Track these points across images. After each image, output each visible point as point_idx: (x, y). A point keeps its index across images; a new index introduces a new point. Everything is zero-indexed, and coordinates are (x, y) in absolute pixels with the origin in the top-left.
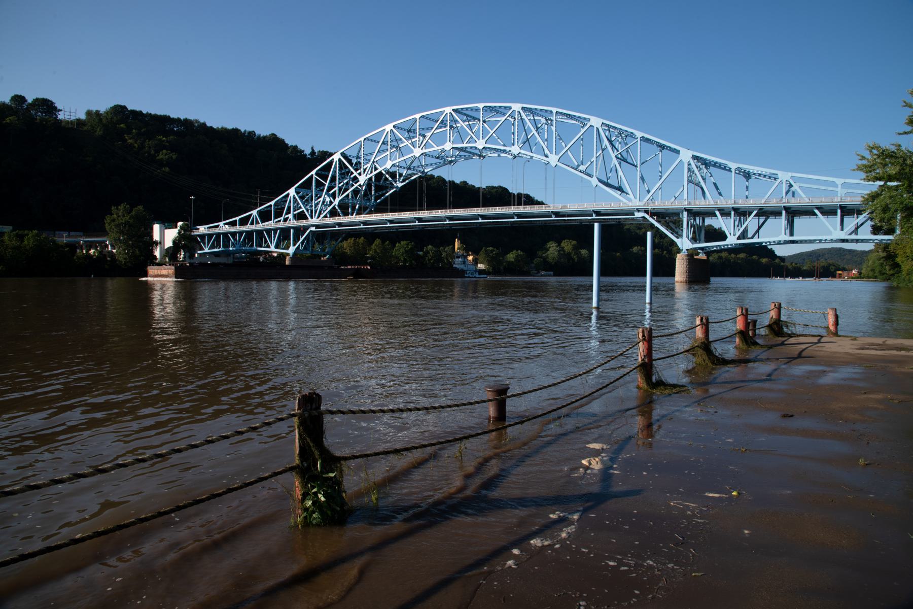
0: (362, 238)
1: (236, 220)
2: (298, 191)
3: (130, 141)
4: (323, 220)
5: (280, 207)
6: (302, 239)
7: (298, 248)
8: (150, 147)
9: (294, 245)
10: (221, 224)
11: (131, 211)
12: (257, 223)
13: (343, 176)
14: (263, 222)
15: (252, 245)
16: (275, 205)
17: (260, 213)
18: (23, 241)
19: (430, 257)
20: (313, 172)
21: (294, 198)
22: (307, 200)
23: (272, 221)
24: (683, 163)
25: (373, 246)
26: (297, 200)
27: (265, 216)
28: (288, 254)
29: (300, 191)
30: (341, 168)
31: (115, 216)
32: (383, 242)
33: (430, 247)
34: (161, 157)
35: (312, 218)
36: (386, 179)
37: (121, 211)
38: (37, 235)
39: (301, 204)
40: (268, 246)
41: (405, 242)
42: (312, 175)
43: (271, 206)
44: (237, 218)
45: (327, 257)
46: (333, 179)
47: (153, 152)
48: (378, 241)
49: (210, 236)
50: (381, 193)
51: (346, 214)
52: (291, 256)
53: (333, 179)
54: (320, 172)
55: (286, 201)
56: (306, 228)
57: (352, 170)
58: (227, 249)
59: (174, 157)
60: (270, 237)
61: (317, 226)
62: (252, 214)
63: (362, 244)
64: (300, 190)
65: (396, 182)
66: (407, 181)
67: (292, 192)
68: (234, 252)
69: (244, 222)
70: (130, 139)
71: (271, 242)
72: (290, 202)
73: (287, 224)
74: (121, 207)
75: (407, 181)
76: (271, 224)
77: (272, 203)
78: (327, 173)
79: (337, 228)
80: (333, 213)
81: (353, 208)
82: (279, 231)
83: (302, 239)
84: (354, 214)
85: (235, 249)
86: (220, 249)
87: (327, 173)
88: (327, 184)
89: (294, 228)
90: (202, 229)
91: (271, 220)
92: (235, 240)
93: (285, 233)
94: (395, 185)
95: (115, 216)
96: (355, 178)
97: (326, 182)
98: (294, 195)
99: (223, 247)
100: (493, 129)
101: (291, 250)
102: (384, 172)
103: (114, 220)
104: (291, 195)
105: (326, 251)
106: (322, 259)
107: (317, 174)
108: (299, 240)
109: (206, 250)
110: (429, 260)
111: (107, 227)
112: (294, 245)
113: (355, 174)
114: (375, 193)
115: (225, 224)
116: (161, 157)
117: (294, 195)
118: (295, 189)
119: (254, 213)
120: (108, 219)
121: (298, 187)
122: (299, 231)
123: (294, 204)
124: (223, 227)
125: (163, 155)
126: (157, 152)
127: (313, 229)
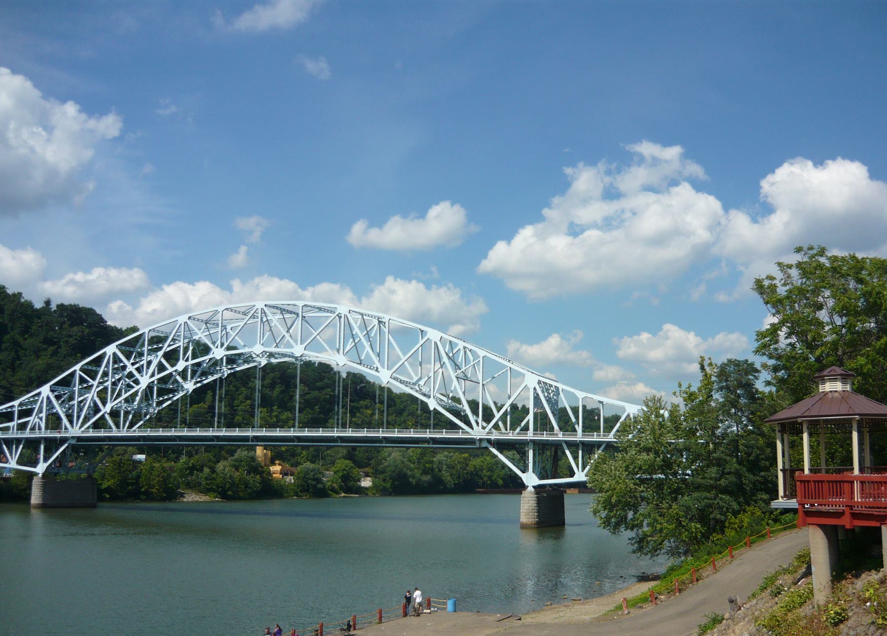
2: (53, 389)
9: (45, 460)
13: (115, 371)
16: (21, 405)
20: (77, 367)
21: (48, 398)
22: (63, 402)
24: (529, 389)
28: (36, 474)
30: (115, 362)
42: (74, 372)
50: (166, 397)
54: (86, 367)
72: (42, 402)
73: (36, 435)
77: (16, 403)
88: (95, 383)
93: (32, 444)
100: (318, 329)
101: (41, 468)
107: (82, 370)
118: (50, 386)
121: (54, 384)
122: (52, 445)
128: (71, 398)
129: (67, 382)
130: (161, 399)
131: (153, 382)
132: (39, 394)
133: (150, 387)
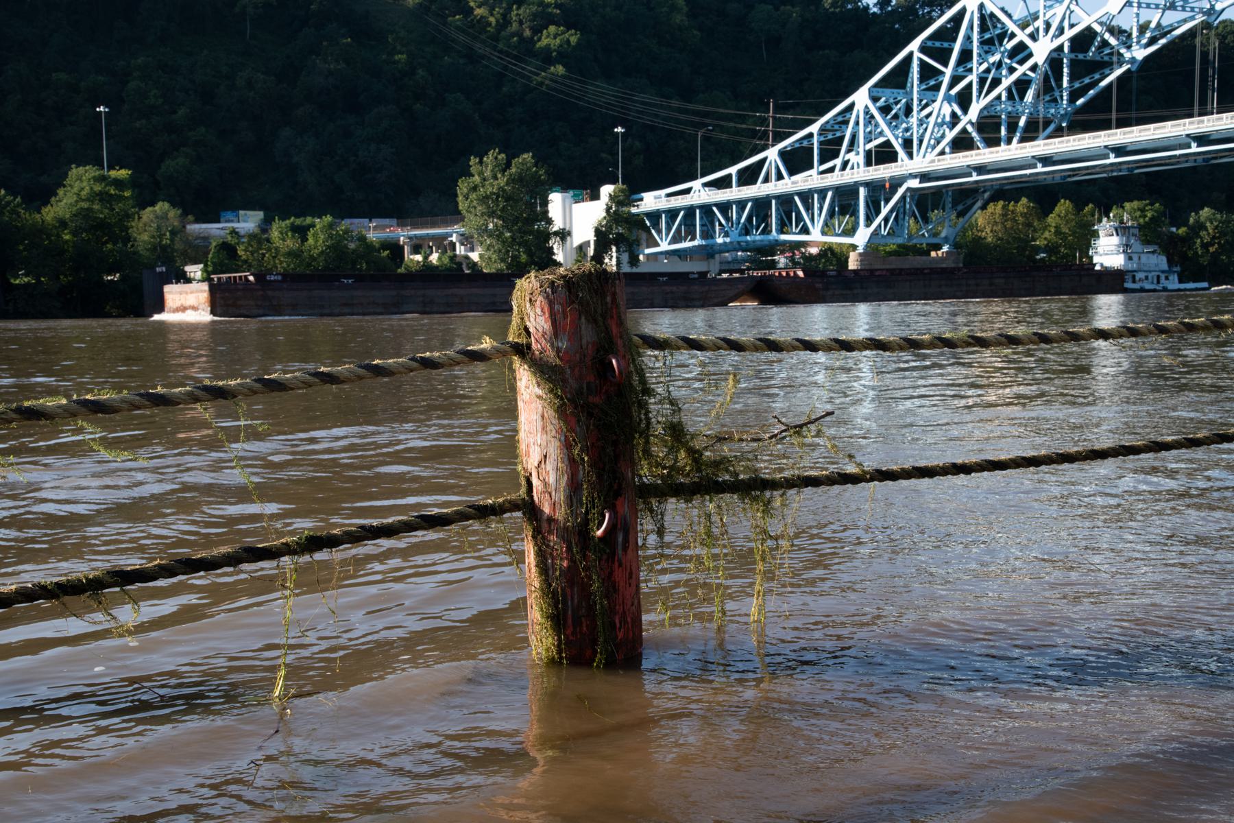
0: (1024, 200)
1: (730, 176)
2: (875, 94)
3: (479, 12)
4: (939, 161)
5: (830, 137)
6: (885, 211)
7: (875, 233)
8: (521, 23)
9: (868, 224)
10: (696, 184)
11: (508, 165)
12: (780, 177)
13: (986, 48)
14: (792, 173)
15: (766, 231)
16: (823, 130)
17: (783, 154)
18: (304, 239)
19: (1207, 239)
20: (914, 46)
22: (896, 117)
23: (813, 172)
25: (1052, 219)
26: (872, 117)
27: (796, 161)
28: (854, 247)
29: (879, 95)
30: (984, 28)
31: (477, 179)
32: (1079, 207)
33: (1206, 212)
34: (545, 41)
35: (910, 156)
36: (1105, 43)
37: (490, 167)
38: (331, 226)
39: (883, 126)
40: (805, 231)
41: (1136, 204)
42: (911, 54)
43: (811, 135)
44: (733, 170)
45: (945, 248)
46: (966, 56)
47: (527, 33)
48: (1064, 206)
49: (672, 214)
50: (1087, 80)
51: (992, 142)
52: (860, 250)
53: (966, 56)
54: (930, 44)
55: (846, 122)
56: (896, 183)
57: (1012, 27)
58: (710, 242)
59: (574, 40)
60: (809, 208)
61: (924, 177)
62: (765, 160)
63: (1024, 215)
64: (876, 92)
65: (1129, 47)
66: (1163, 41)
67: (861, 98)
68: (725, 248)
69: (748, 177)
70: (479, 7)
71: (812, 220)
73: (847, 177)
74: (489, 159)
75: (1163, 41)
76: (809, 179)
77: (814, 128)
78: (946, 45)
79: (975, 177)
80: (962, 143)
81: (1012, 128)
82: (830, 194)
83: (885, 211)
84: (1015, 140)
85: (728, 240)
86: (695, 243)
87: (946, 45)
88: (948, 72)
89: (867, 184)
90: (651, 201)
91: (811, 167)
92: (728, 219)
93: (844, 199)
94: (1127, 55)
95: (477, 179)
96: (1021, 47)
97: (946, 65)
98: (866, 107)
99: (703, 237)
101: (862, 237)
102: (1098, 28)
103: (475, 188)
104: (860, 107)
105: (943, 235)
106: (933, 254)
107: (923, 49)
108: (878, 212)
109: (664, 246)
110: (1205, 246)
111: (462, 205)
112: (868, 224)
113: (1022, 36)
114: (1071, 81)
115: (705, 185)
116: (545, 41)
117: (866, 107)
119: (772, 154)
120: (463, 186)
121: (876, 85)
123: (865, 126)
124: (699, 193)
125: (550, 38)
126: (537, 31)
127: (914, 183)
128: (908, 111)
129: (898, 78)
130: (1077, 85)
131: (1060, 48)
132: (851, 107)
133: (1054, 61)
